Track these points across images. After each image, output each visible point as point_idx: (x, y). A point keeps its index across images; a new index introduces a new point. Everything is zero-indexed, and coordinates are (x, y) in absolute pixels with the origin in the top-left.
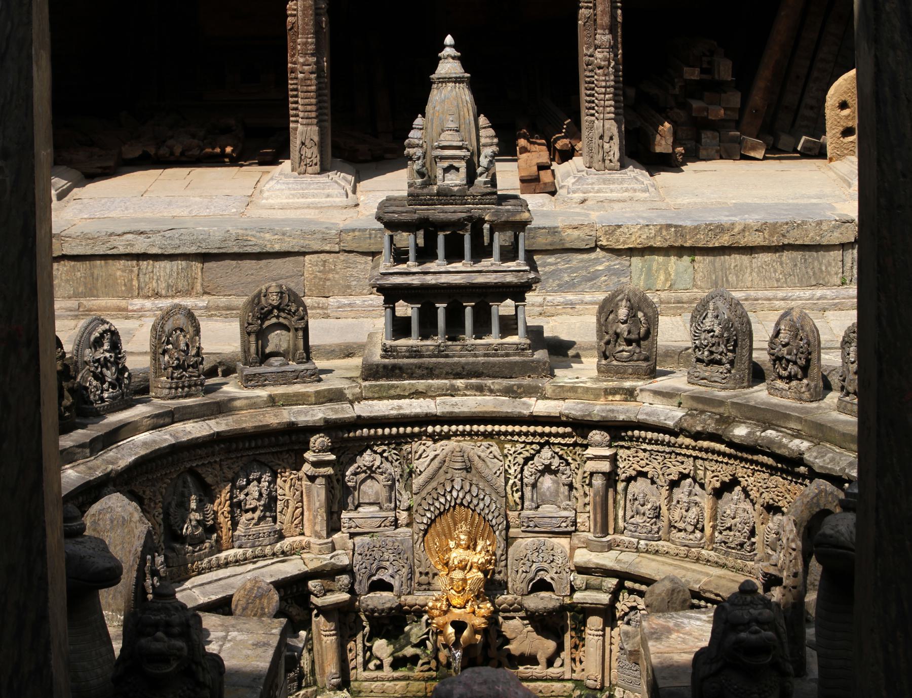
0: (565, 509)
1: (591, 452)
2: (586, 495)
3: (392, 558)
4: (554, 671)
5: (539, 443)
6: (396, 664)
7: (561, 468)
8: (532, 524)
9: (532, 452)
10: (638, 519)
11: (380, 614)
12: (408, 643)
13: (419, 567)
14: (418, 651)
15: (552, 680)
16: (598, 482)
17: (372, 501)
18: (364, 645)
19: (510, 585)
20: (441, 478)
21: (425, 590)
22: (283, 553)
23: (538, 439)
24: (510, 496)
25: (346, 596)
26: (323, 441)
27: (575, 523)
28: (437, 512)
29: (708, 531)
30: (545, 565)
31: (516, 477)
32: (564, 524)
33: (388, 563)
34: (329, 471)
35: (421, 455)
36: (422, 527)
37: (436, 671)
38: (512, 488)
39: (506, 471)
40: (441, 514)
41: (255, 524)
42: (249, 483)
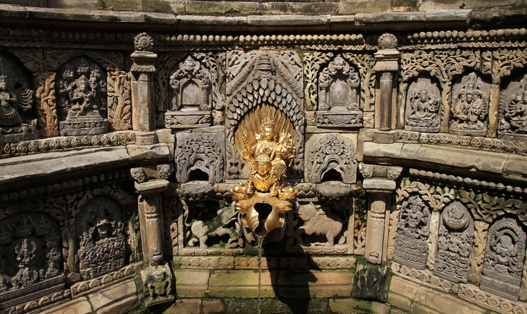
1: (380, 53)
2: (371, 96)
4: (339, 247)
6: (211, 241)
7: (350, 73)
8: (326, 121)
10: (418, 115)
11: (194, 198)
12: (220, 224)
13: (230, 158)
14: (228, 231)
15: (338, 255)
16: (386, 80)
18: (185, 227)
19: (306, 175)
20: (250, 78)
21: (235, 178)
22: (110, 143)
23: (332, 47)
24: (307, 98)
25: (164, 183)
26: (145, 39)
27: (362, 121)
28: (246, 109)
29: (492, 119)
30: (337, 157)
31: (313, 81)
33: (204, 155)
34: (153, 69)
36: (233, 122)
37: (243, 248)
38: (309, 91)
40: (249, 111)
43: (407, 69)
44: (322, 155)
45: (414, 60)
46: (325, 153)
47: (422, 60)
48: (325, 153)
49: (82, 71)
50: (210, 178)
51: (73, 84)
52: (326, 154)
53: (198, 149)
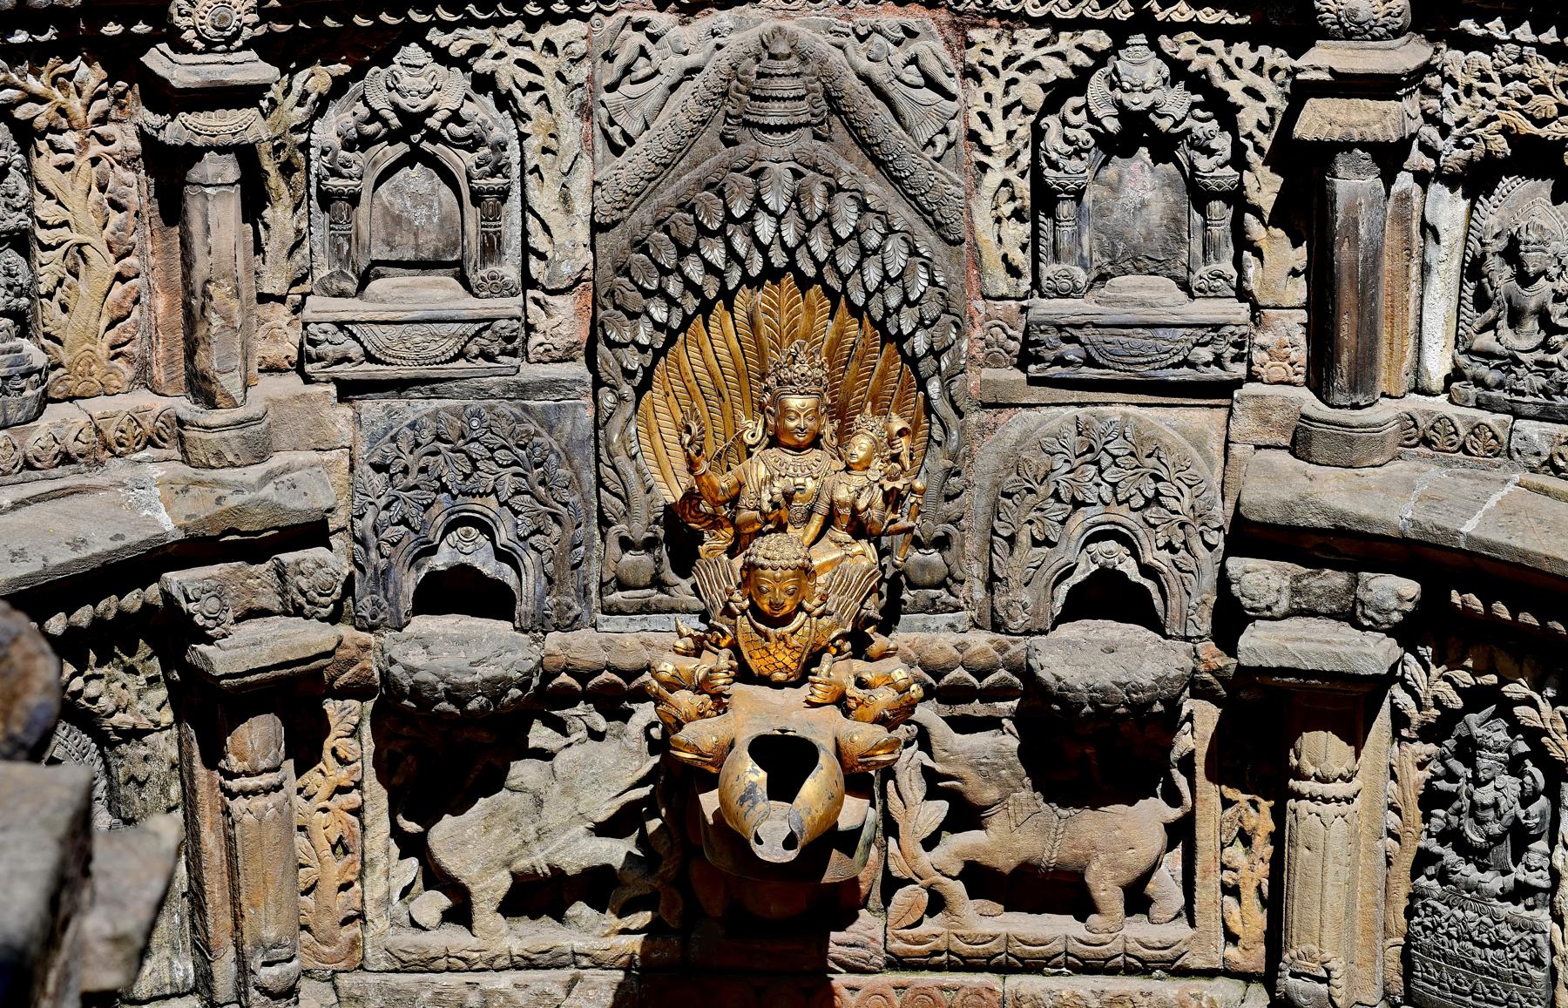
0: (1208, 293)
3: (508, 482)
5: (1109, 26)
8: (1071, 352)
9: (1082, 59)
17: (426, 255)
22: (66, 459)
28: (691, 304)
31: (1011, 161)
32: (1206, 354)
35: (627, 70)
39: (973, 136)
43: (1459, 124)
44: (1056, 510)
45: (1495, 88)
50: (521, 608)
53: (466, 477)
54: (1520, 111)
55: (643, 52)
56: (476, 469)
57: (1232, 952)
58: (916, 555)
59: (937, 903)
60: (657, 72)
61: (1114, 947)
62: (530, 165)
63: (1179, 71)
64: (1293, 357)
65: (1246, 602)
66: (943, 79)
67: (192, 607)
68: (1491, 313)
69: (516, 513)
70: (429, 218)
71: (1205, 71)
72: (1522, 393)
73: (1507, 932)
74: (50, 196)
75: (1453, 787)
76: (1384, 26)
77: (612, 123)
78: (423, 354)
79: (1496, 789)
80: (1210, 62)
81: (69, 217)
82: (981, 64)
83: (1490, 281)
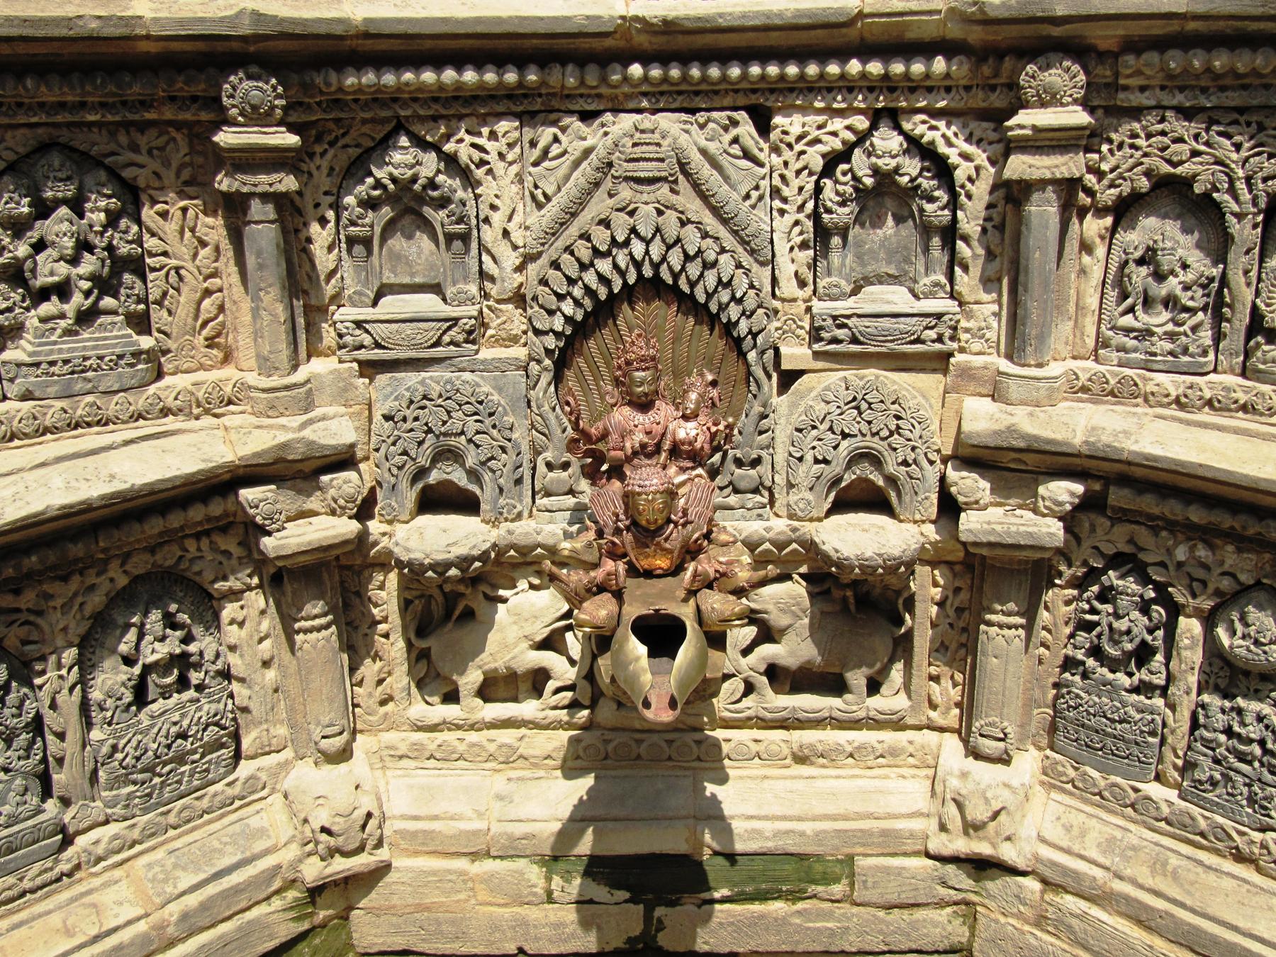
0: (929, 295)
8: (841, 333)
9: (851, 137)
30: (875, 443)
32: (932, 334)
34: (288, 183)
35: (546, 152)
39: (775, 192)
41: (68, 332)
42: (43, 210)
43: (1112, 171)
45: (1141, 142)
46: (837, 430)
47: (1166, 140)
48: (838, 431)
49: (60, 195)
50: (483, 506)
51: (33, 235)
52: (845, 436)
53: (444, 423)
54: (1162, 158)
55: (556, 140)
56: (451, 417)
57: (933, 714)
58: (738, 471)
59: (749, 688)
60: (565, 153)
61: (862, 714)
62: (482, 216)
63: (915, 145)
64: (988, 336)
65: (961, 499)
66: (756, 152)
67: (252, 511)
68: (1130, 301)
69: (478, 446)
70: (419, 254)
71: (932, 143)
72: (1155, 354)
73: (1132, 712)
74: (153, 235)
75: (1095, 618)
76: (1071, 96)
77: (536, 187)
78: (413, 342)
79: (1131, 621)
80: (936, 135)
81: (168, 248)
82: (781, 141)
83: (1130, 279)
